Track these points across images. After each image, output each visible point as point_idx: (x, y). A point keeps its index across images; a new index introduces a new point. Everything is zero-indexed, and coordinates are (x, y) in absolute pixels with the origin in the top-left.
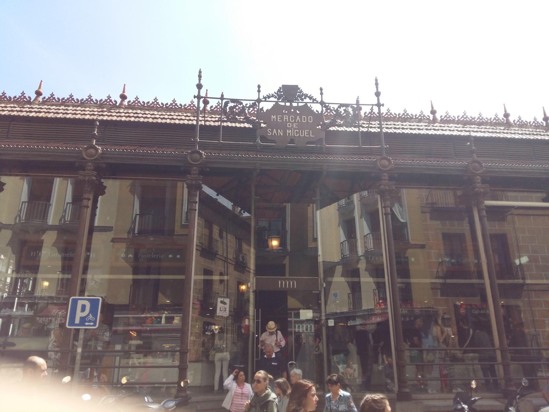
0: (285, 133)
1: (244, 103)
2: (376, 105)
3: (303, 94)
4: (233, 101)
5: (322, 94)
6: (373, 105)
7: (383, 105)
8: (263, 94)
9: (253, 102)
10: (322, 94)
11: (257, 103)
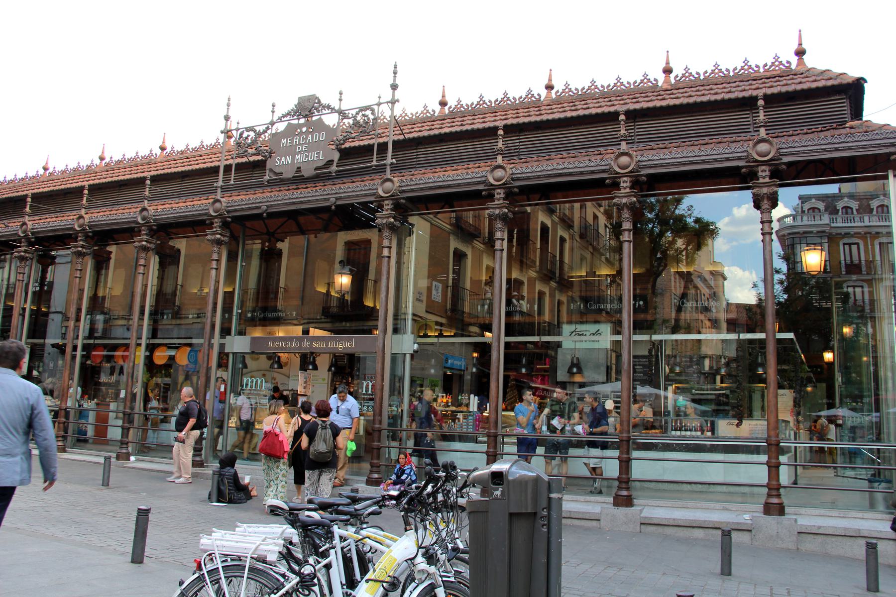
0: (293, 159)
5: (340, 100)
8: (279, 113)
10: (340, 100)
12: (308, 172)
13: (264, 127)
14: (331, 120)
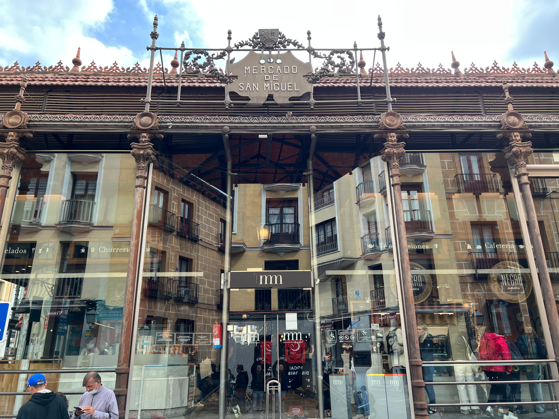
1: (210, 53)
2: (379, 49)
3: (285, 41)
4: (196, 51)
5: (309, 39)
6: (375, 49)
7: (388, 49)
8: (235, 41)
9: (222, 51)
10: (309, 39)
11: (226, 53)
12: (281, 99)
13: (219, 52)
14: (302, 56)
